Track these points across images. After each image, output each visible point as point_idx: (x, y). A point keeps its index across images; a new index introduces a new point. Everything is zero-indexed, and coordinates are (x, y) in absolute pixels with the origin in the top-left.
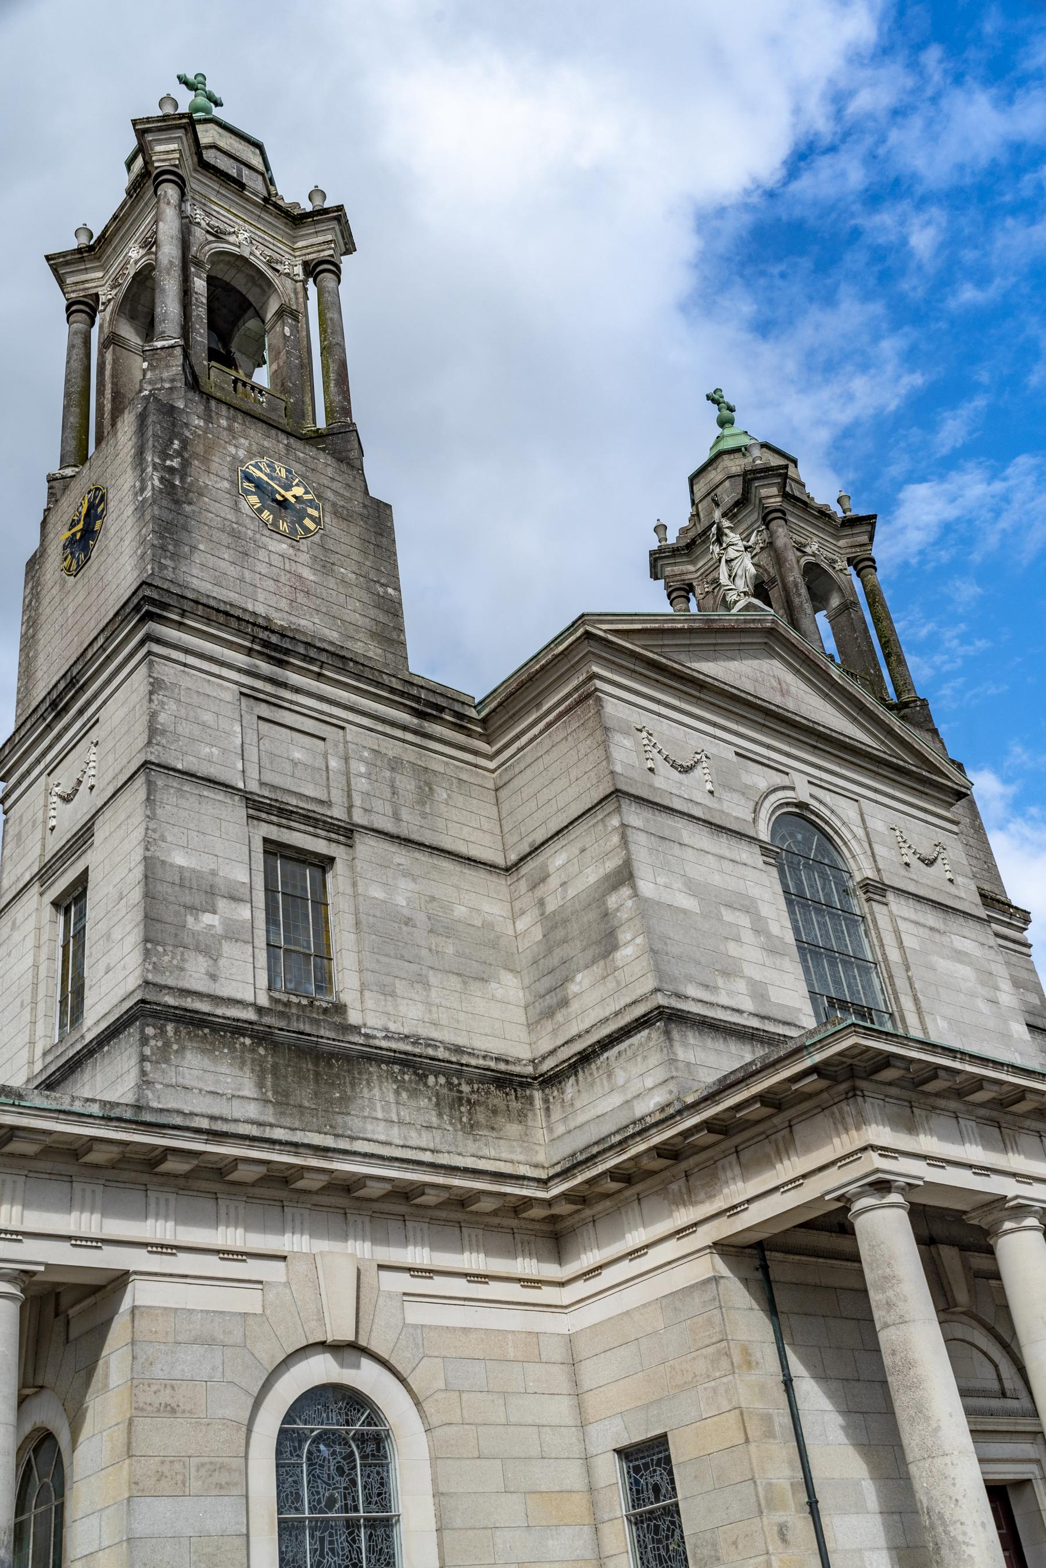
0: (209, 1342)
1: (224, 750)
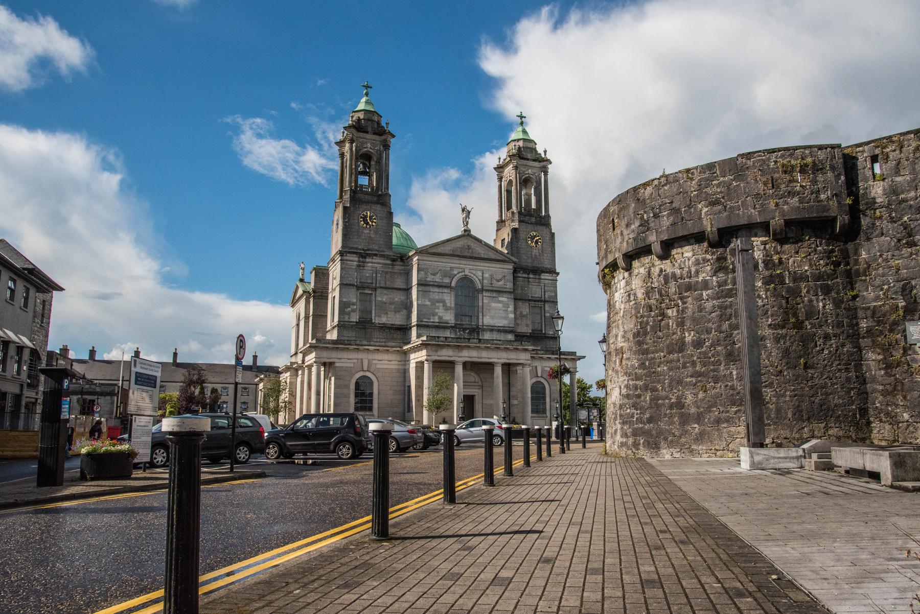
0: (346, 371)
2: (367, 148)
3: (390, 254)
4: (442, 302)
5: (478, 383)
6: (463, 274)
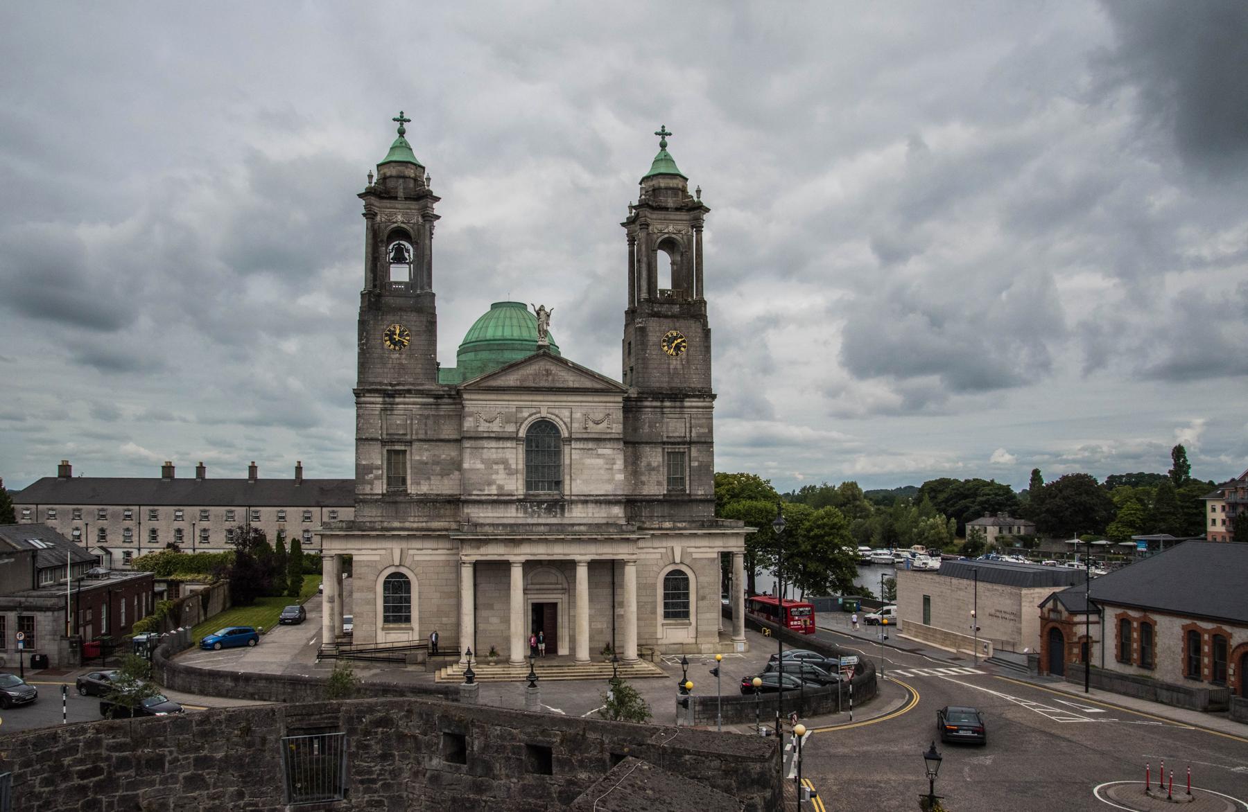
0: (368, 566)
1: (376, 430)
2: (396, 222)
3: (433, 388)
4: (503, 463)
5: (562, 584)
6: (538, 415)
